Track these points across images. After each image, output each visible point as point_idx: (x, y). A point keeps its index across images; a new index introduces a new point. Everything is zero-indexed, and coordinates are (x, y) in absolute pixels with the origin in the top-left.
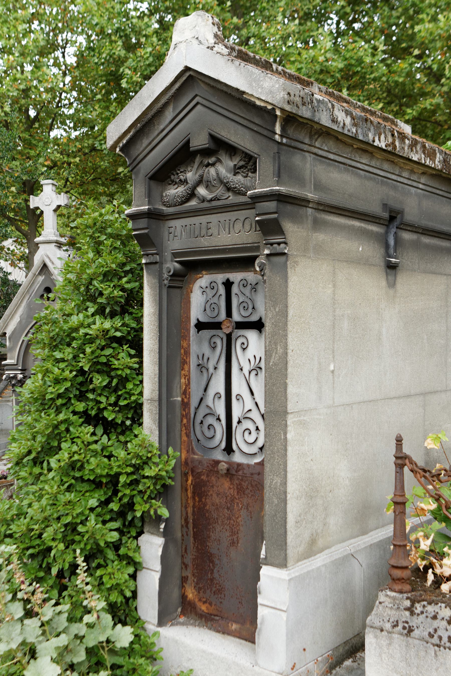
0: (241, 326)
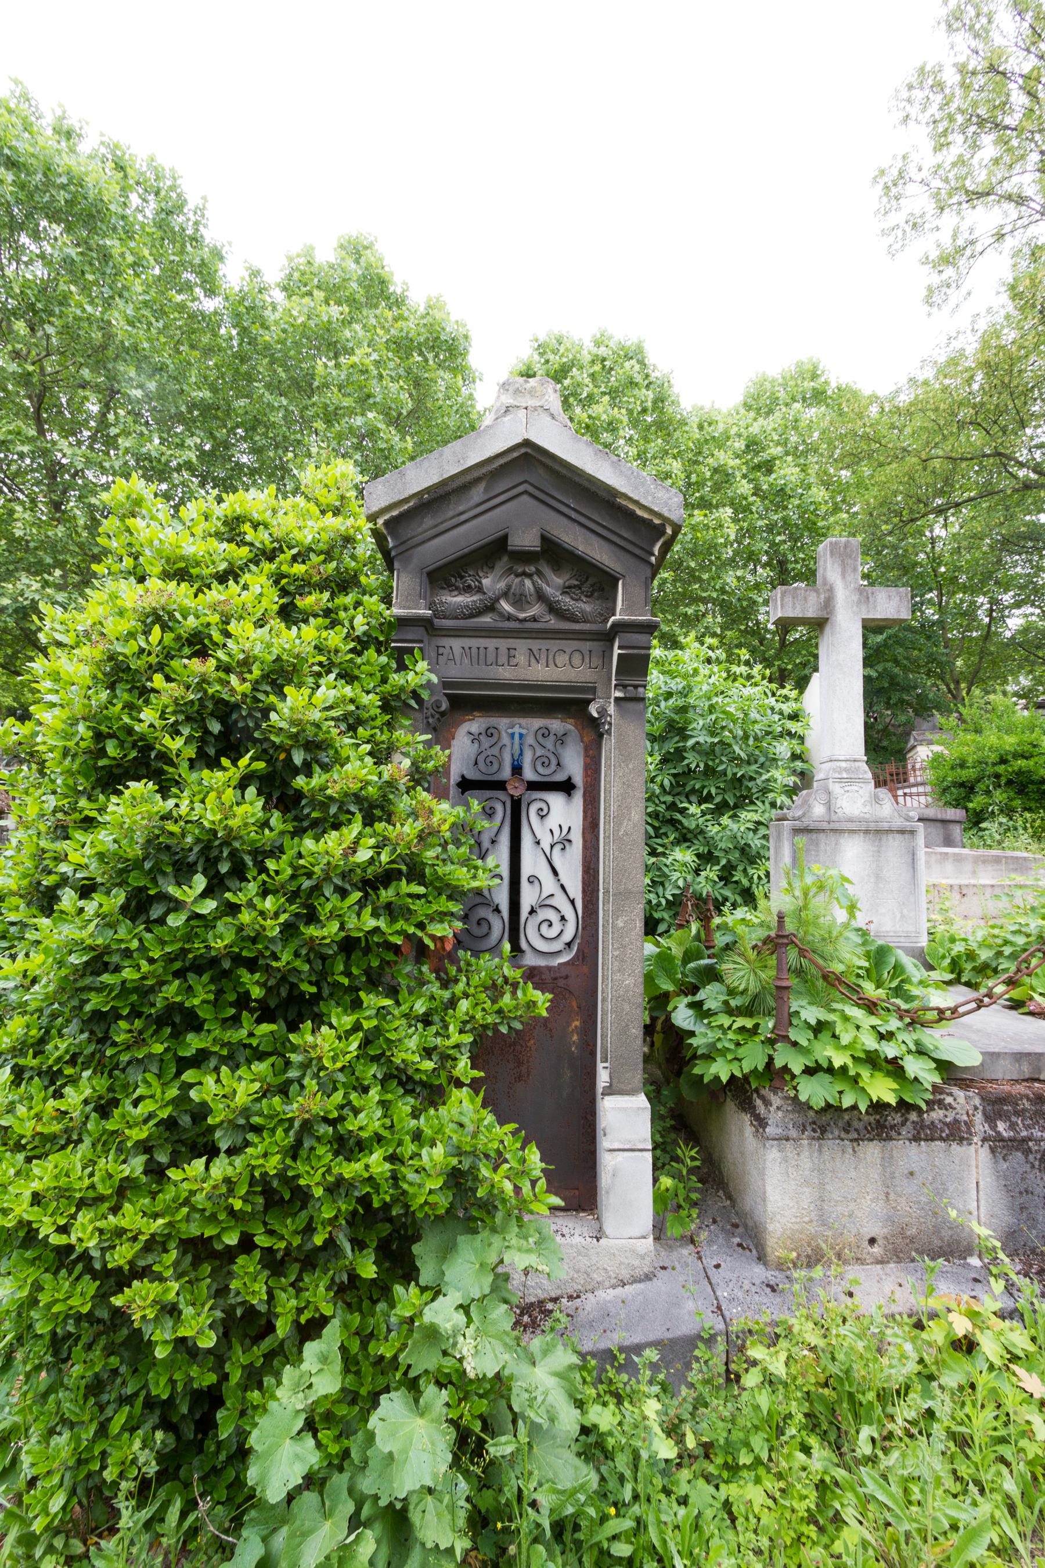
0: (533, 786)
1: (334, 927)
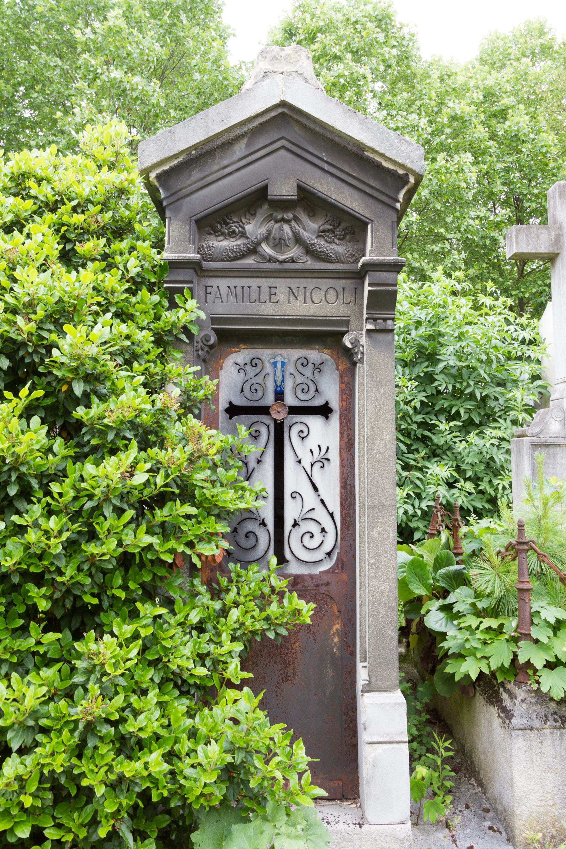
0: (294, 411)
1: (112, 543)
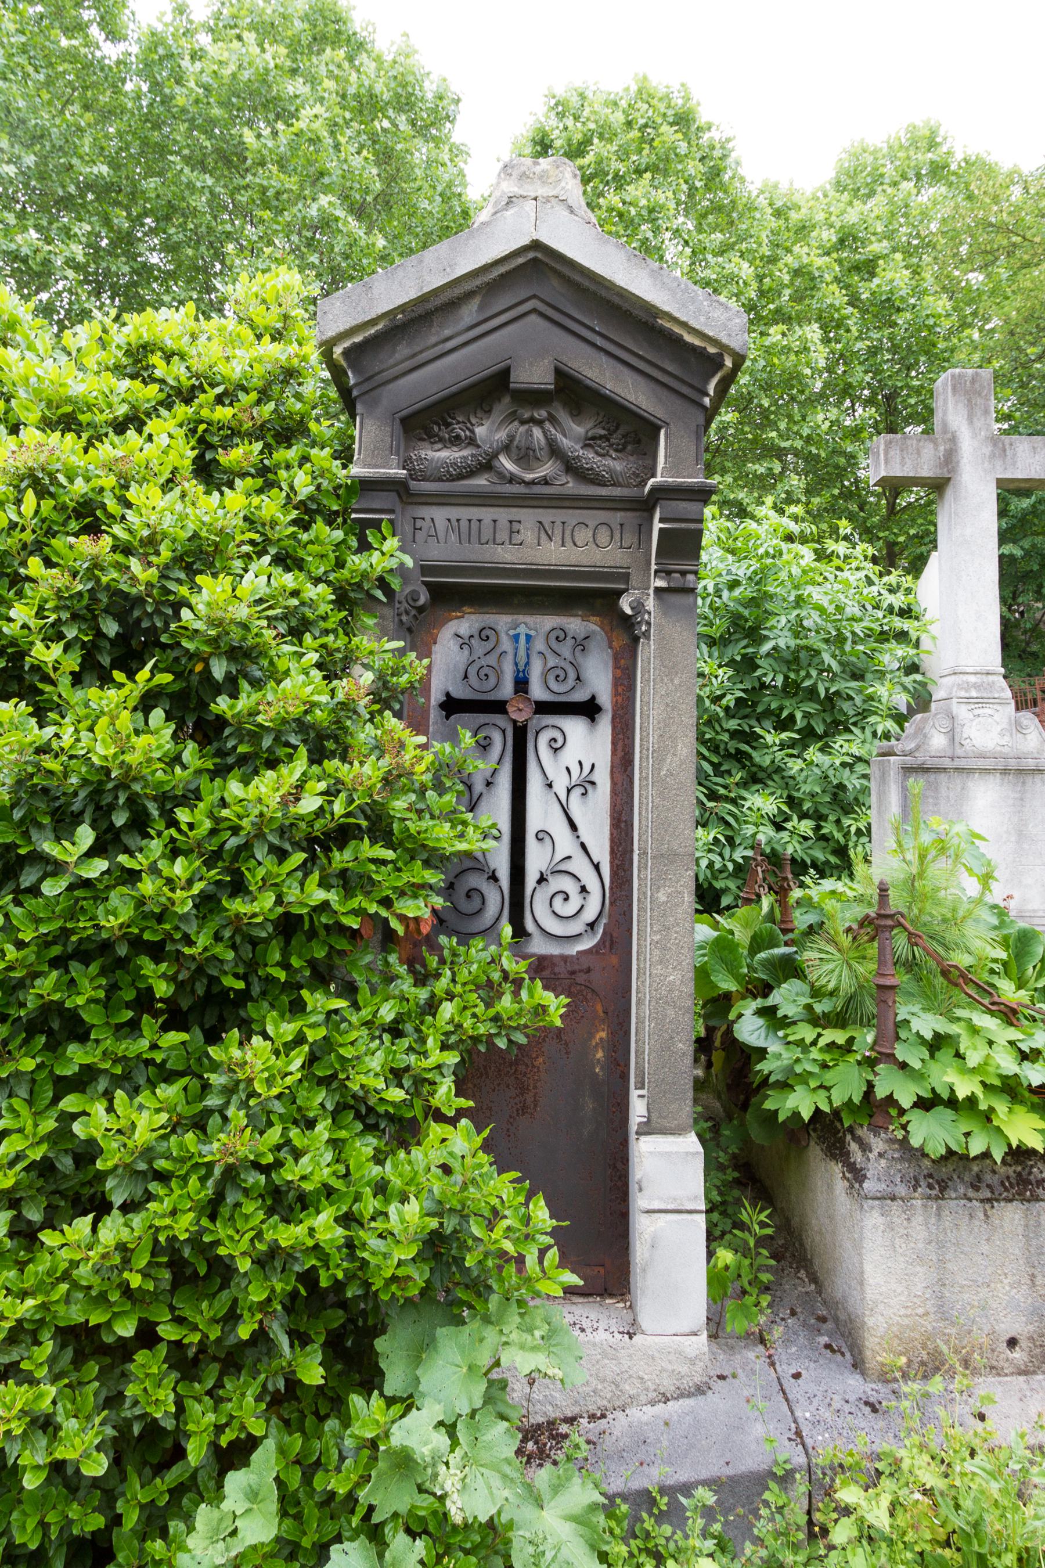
0: (544, 708)
1: (269, 899)
